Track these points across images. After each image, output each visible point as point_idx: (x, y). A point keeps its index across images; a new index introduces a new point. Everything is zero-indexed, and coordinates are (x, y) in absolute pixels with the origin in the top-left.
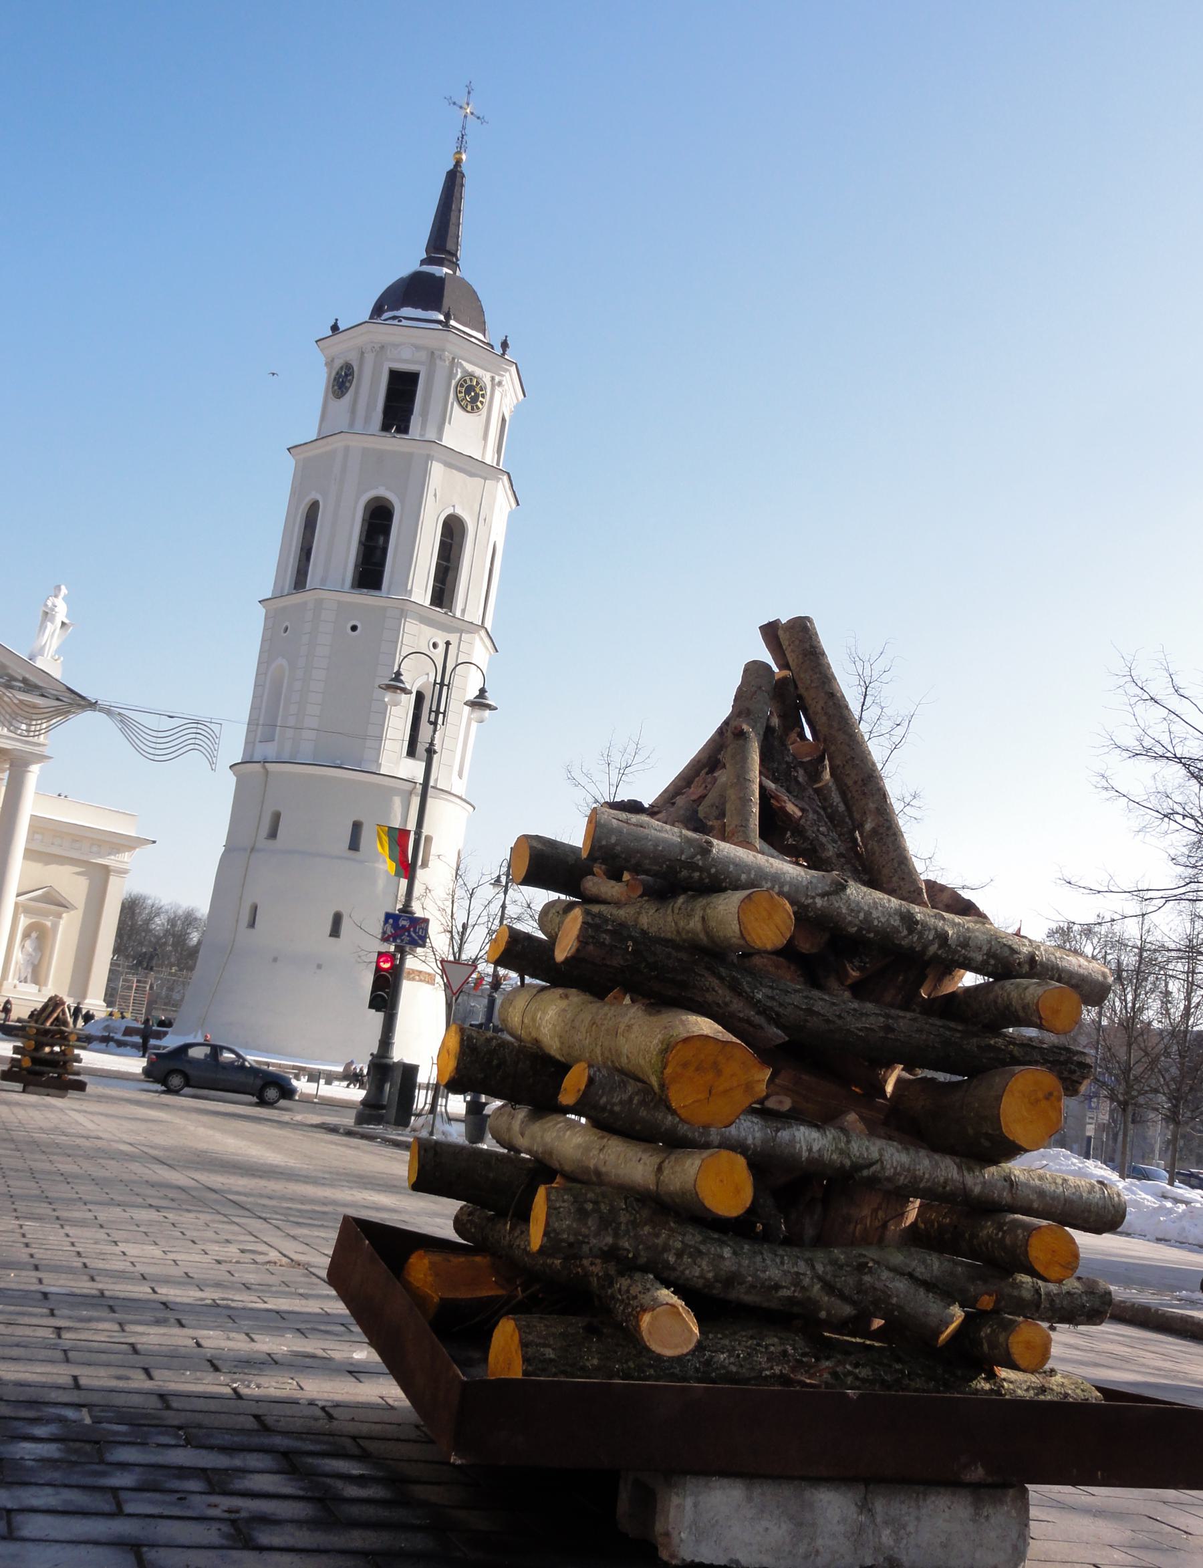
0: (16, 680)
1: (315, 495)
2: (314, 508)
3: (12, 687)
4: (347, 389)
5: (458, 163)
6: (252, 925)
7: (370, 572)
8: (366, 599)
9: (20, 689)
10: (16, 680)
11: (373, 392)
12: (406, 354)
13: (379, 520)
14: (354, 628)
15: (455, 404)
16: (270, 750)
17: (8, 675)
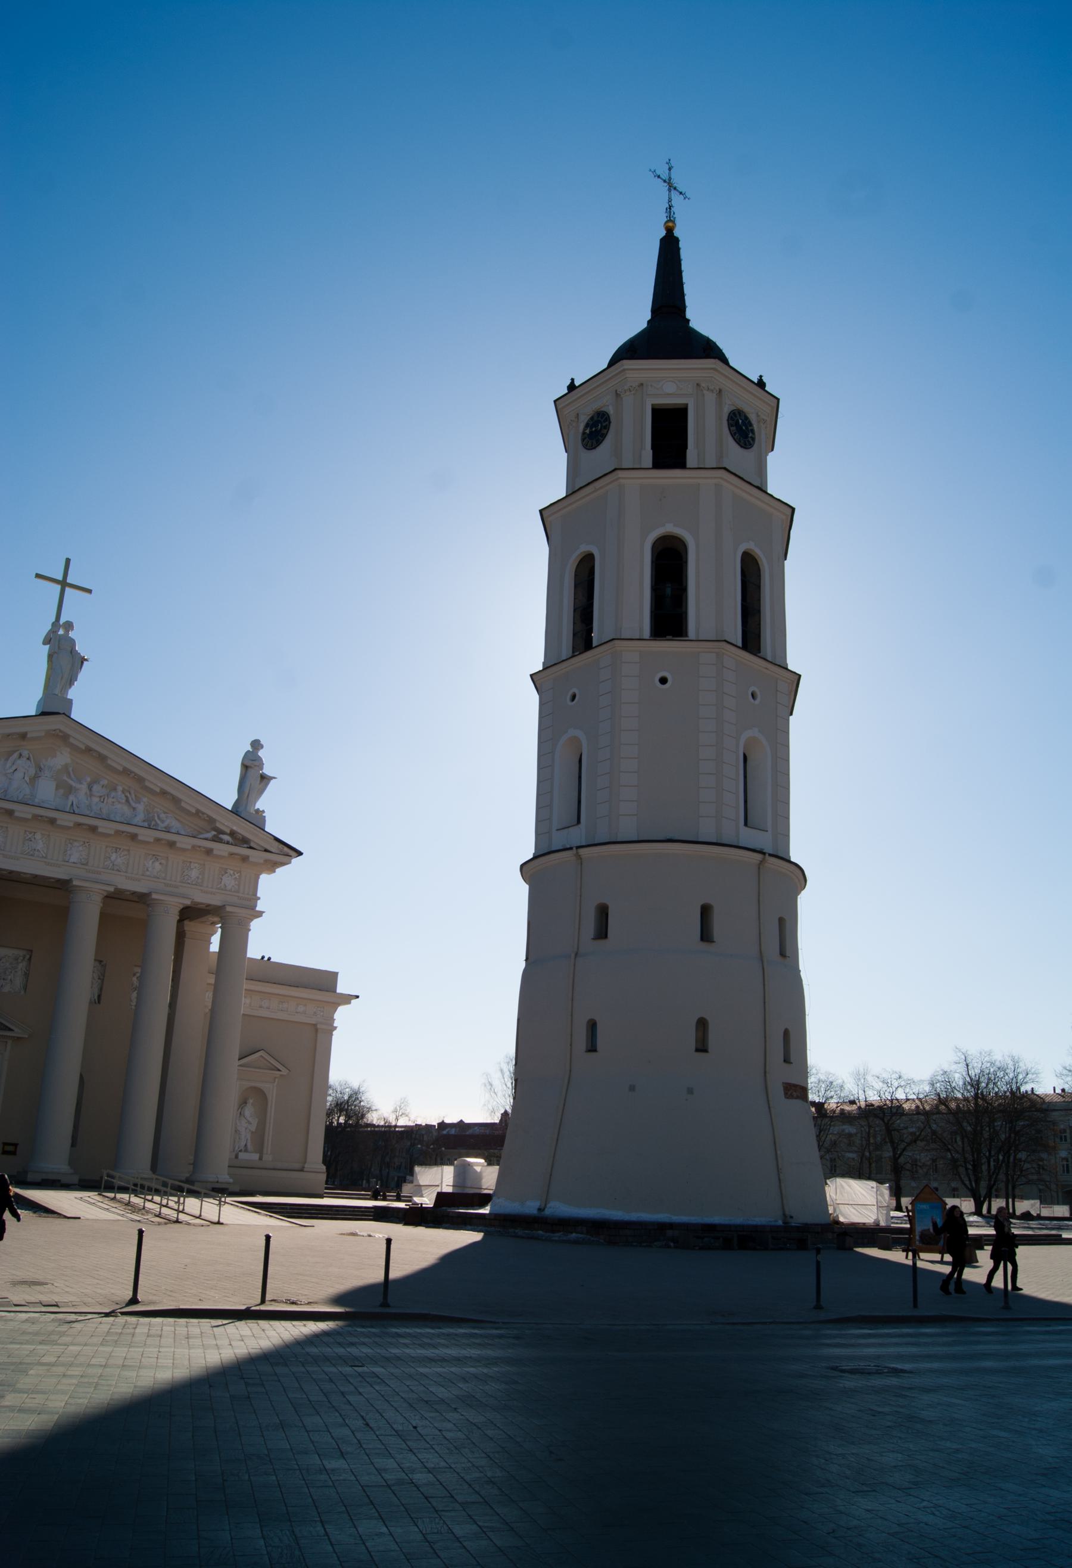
0: (224, 833)
1: (584, 548)
3: (221, 841)
4: (604, 436)
5: (670, 231)
6: (592, 1048)
7: (669, 619)
8: (669, 646)
9: (228, 843)
10: (224, 833)
11: (634, 434)
12: (670, 388)
13: (669, 562)
14: (663, 681)
16: (577, 835)
17: (216, 829)
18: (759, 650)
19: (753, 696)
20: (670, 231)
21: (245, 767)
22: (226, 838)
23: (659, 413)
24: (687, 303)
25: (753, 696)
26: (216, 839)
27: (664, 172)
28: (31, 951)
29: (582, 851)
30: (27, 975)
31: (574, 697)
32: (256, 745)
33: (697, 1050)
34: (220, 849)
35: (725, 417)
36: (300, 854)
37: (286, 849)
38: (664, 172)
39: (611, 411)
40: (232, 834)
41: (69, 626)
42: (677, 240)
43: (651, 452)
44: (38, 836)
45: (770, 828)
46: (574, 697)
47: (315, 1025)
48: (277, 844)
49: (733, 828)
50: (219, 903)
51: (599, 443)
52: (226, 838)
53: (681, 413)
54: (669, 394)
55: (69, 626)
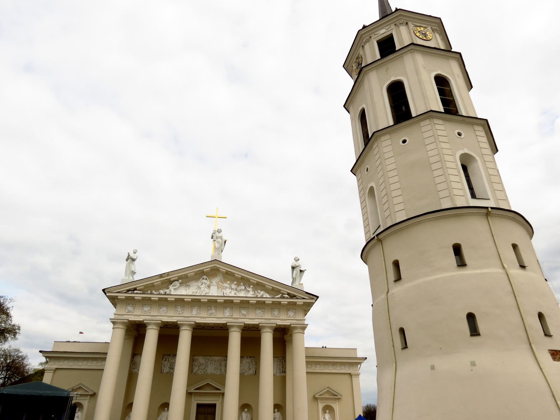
2: (363, 116)
3: (284, 298)
13: (397, 92)
14: (404, 141)
15: (417, 38)
18: (457, 112)
19: (459, 134)
21: (293, 268)
22: (286, 296)
25: (459, 134)
29: (380, 237)
32: (297, 260)
33: (472, 335)
35: (412, 31)
36: (318, 297)
37: (311, 296)
40: (288, 294)
41: (219, 231)
44: (213, 307)
45: (490, 196)
47: (350, 374)
48: (307, 295)
49: (463, 199)
50: (289, 324)
52: (286, 296)
54: (383, 33)
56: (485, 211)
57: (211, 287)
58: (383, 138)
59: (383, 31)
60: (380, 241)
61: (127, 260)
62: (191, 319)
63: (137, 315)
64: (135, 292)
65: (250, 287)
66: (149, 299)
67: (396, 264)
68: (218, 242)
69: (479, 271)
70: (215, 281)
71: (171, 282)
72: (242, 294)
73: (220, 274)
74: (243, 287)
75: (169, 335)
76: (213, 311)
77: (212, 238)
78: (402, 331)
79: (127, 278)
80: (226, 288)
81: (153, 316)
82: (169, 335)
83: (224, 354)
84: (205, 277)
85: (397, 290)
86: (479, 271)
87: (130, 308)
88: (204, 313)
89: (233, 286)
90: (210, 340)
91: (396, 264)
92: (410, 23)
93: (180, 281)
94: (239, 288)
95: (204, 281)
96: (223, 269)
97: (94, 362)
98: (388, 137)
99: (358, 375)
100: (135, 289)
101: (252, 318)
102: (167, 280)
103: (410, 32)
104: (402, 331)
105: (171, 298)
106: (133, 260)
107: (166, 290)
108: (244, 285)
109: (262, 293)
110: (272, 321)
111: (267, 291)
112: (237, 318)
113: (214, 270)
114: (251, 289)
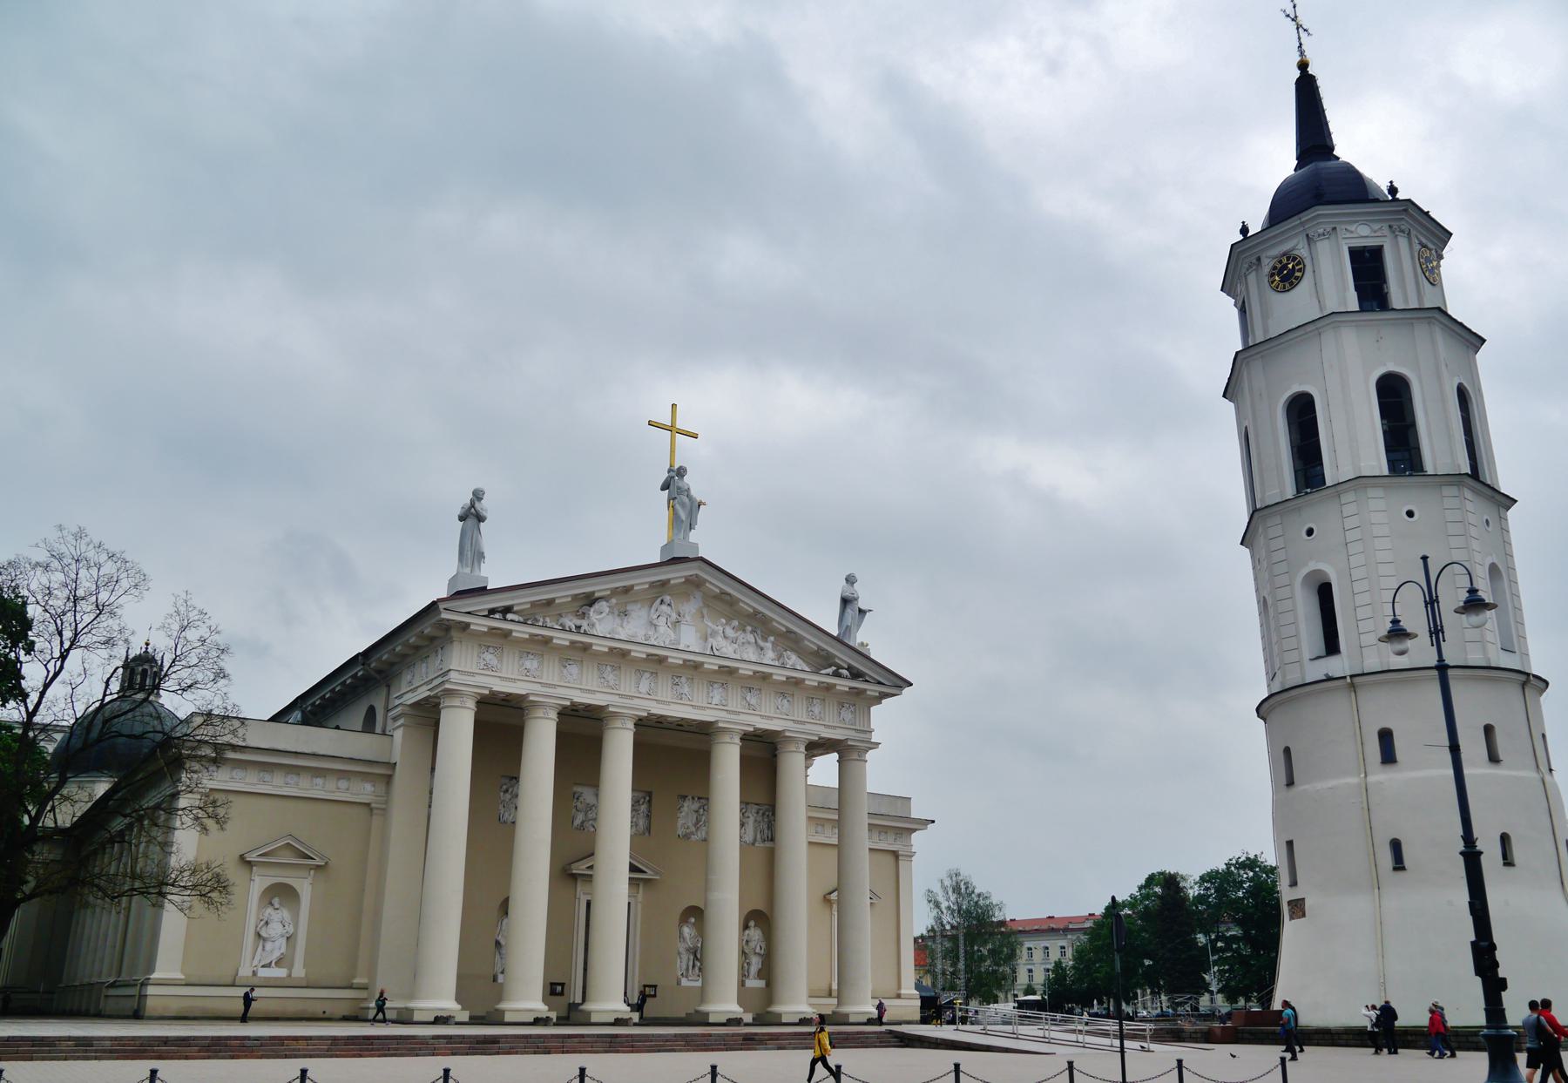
4: (1299, 279)
5: (1303, 66)
20: (1303, 66)
21: (846, 602)
23: (1357, 255)
24: (1335, 141)
26: (836, 674)
27: (1290, 11)
28: (650, 794)
29: (1356, 680)
30: (648, 816)
31: (1310, 532)
32: (850, 580)
34: (843, 685)
38: (1290, 11)
39: (1302, 251)
40: (850, 668)
41: (681, 472)
42: (1312, 79)
43: (1355, 294)
46: (1310, 532)
51: (1293, 286)
52: (845, 672)
53: (1376, 253)
55: (681, 472)
56: (1523, 678)
57: (683, 627)
58: (1371, 493)
59: (1364, 230)
60: (1353, 686)
61: (462, 518)
62: (636, 701)
63: (508, 676)
64: (510, 616)
65: (765, 639)
66: (547, 641)
67: (1386, 737)
68: (683, 505)
69: (1514, 773)
70: (690, 608)
71: (590, 600)
72: (751, 655)
73: (698, 595)
74: (751, 638)
75: (581, 734)
76: (686, 690)
77: (665, 486)
78: (1396, 846)
79: (468, 570)
80: (714, 634)
81: (548, 685)
82: (581, 734)
83: (704, 799)
84: (667, 599)
85: (1381, 776)
86: (1514, 773)
87: (489, 657)
88: (664, 690)
89: (730, 632)
90: (674, 756)
91: (1386, 737)
92: (1413, 232)
93: (614, 601)
94: (741, 636)
95: (664, 608)
96: (715, 584)
97: (319, 781)
98: (1379, 492)
99: (911, 856)
100: (508, 610)
101: (768, 715)
102: (585, 594)
103: (1412, 258)
104: (1396, 846)
105: (601, 646)
106: (480, 519)
107: (579, 622)
108: (753, 632)
109: (794, 657)
110: (808, 727)
111: (802, 653)
112: (738, 713)
113: (685, 578)
114: (769, 645)
